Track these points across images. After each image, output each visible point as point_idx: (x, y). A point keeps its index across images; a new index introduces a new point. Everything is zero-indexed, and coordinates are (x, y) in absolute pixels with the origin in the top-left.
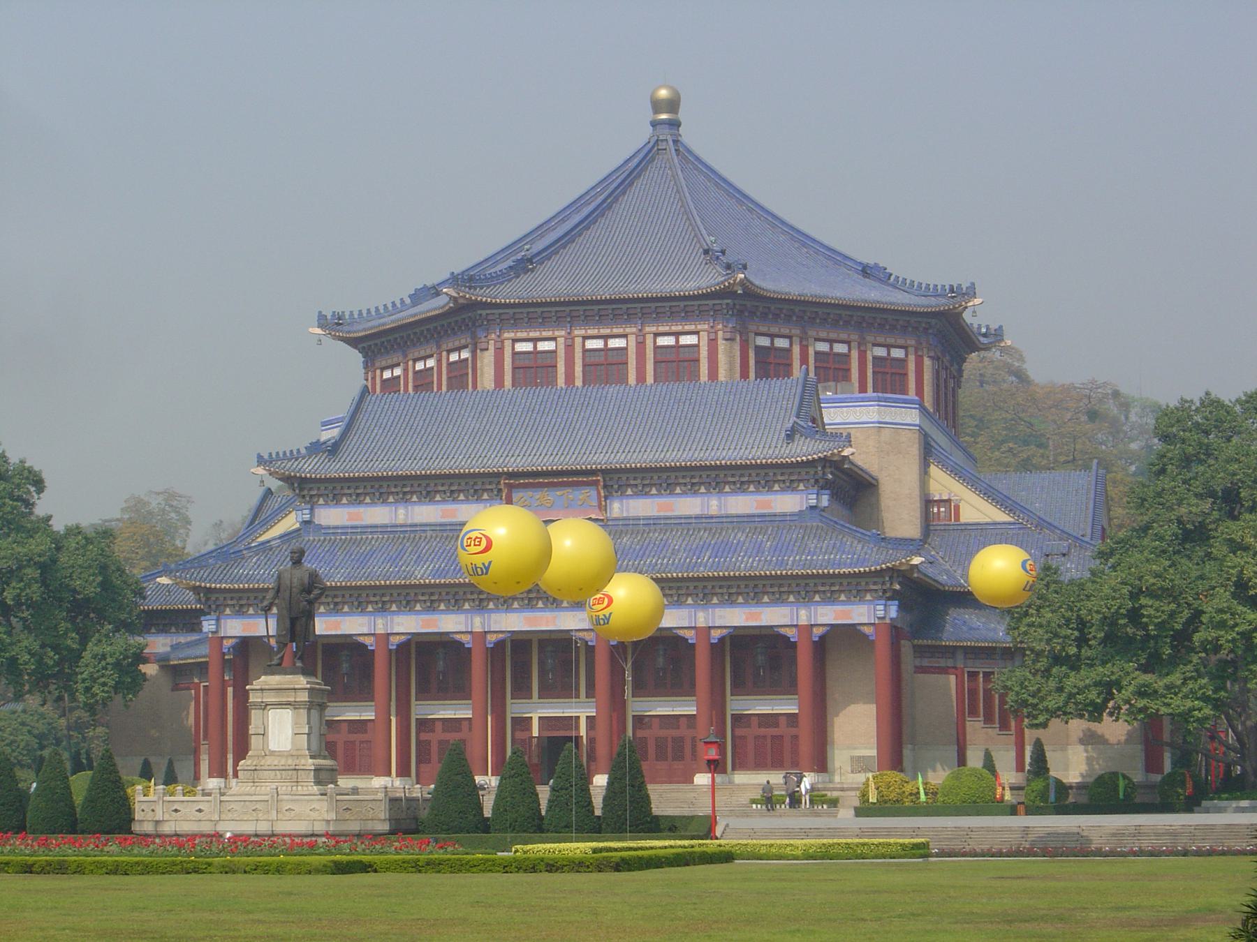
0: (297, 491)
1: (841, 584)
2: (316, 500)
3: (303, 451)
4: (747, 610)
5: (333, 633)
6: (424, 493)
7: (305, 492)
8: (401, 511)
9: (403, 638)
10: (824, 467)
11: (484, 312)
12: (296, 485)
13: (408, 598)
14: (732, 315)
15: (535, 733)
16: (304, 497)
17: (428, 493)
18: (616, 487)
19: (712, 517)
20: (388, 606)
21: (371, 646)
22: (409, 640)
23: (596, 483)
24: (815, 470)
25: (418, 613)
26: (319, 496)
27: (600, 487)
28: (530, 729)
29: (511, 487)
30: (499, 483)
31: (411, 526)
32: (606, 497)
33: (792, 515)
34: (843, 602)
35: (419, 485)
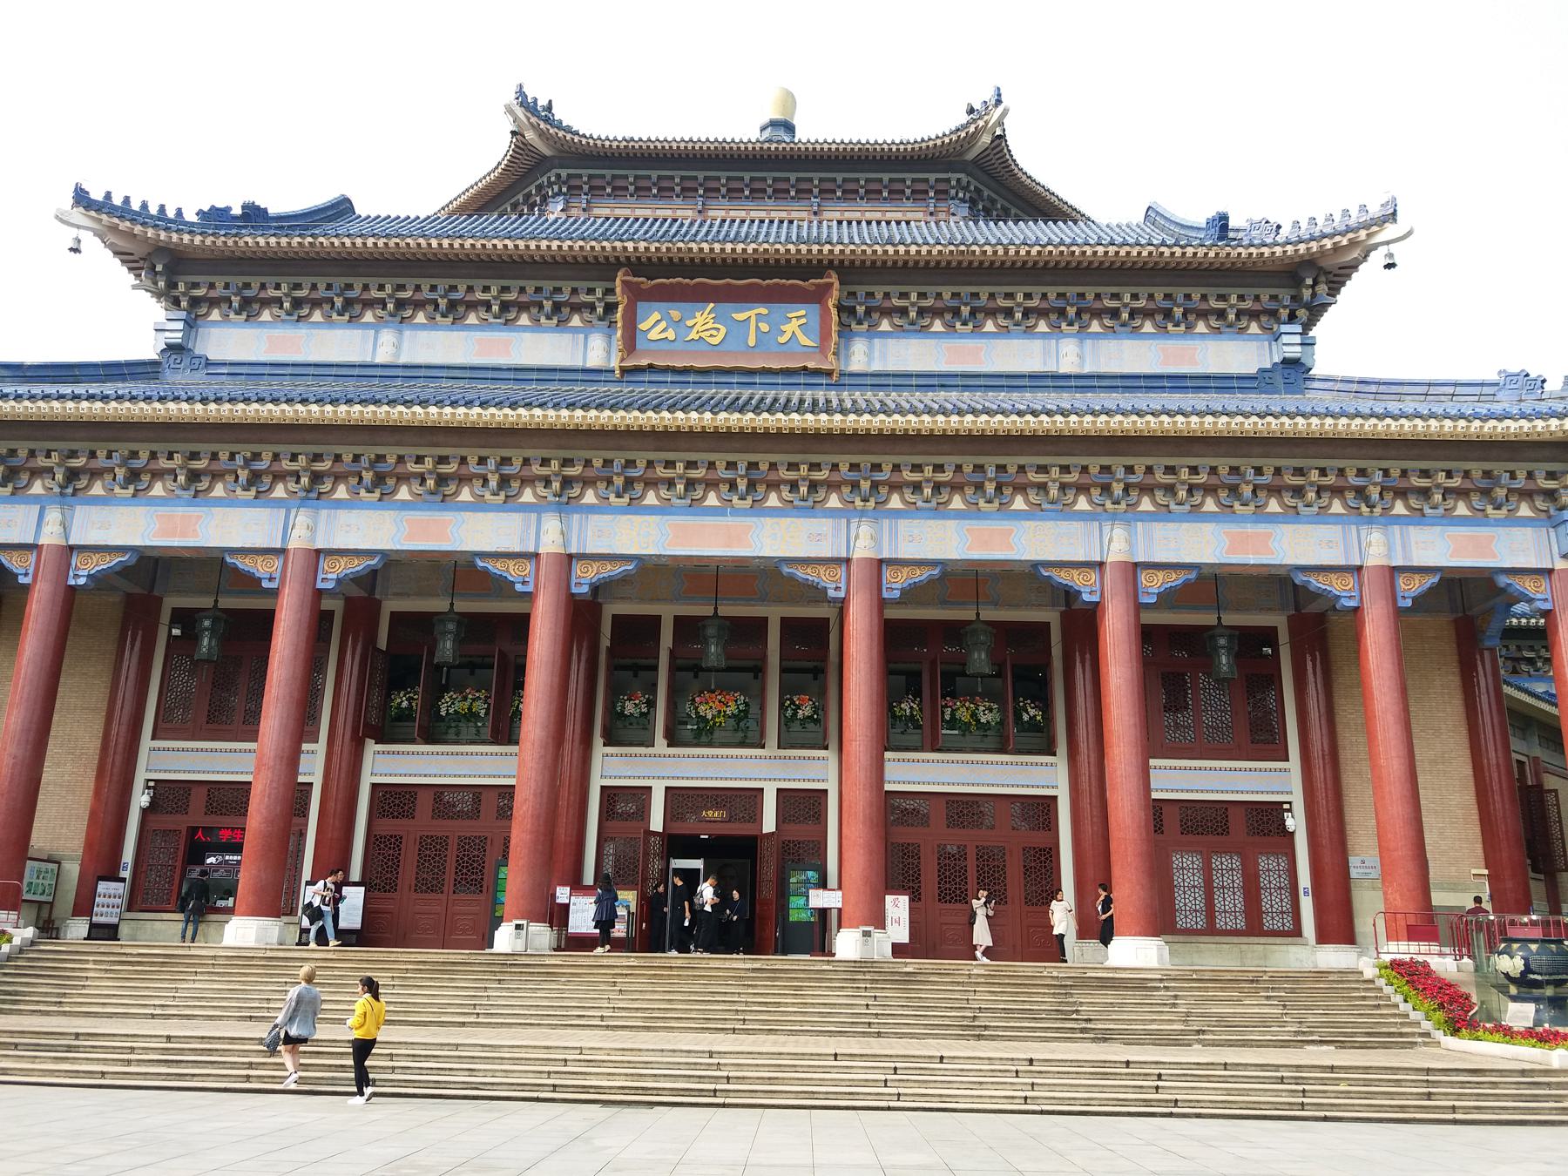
0: (161, 284)
1: (1466, 474)
2: (203, 310)
3: (190, 216)
4: (1234, 528)
5: (176, 542)
6: (443, 303)
7: (181, 287)
8: (387, 336)
9: (357, 566)
10: (1315, 283)
11: (564, 173)
12: (159, 268)
13: (381, 467)
14: (963, 200)
15: (657, 823)
16: (176, 302)
17: (452, 305)
18: (861, 310)
19: (1068, 377)
20: (326, 486)
21: (271, 579)
22: (373, 573)
23: (818, 296)
24: (1293, 292)
25: (404, 505)
26: (213, 303)
27: (831, 303)
28: (644, 812)
29: (638, 295)
30: (610, 291)
31: (405, 367)
32: (840, 334)
33: (1240, 378)
34: (1463, 521)
35: (433, 288)
